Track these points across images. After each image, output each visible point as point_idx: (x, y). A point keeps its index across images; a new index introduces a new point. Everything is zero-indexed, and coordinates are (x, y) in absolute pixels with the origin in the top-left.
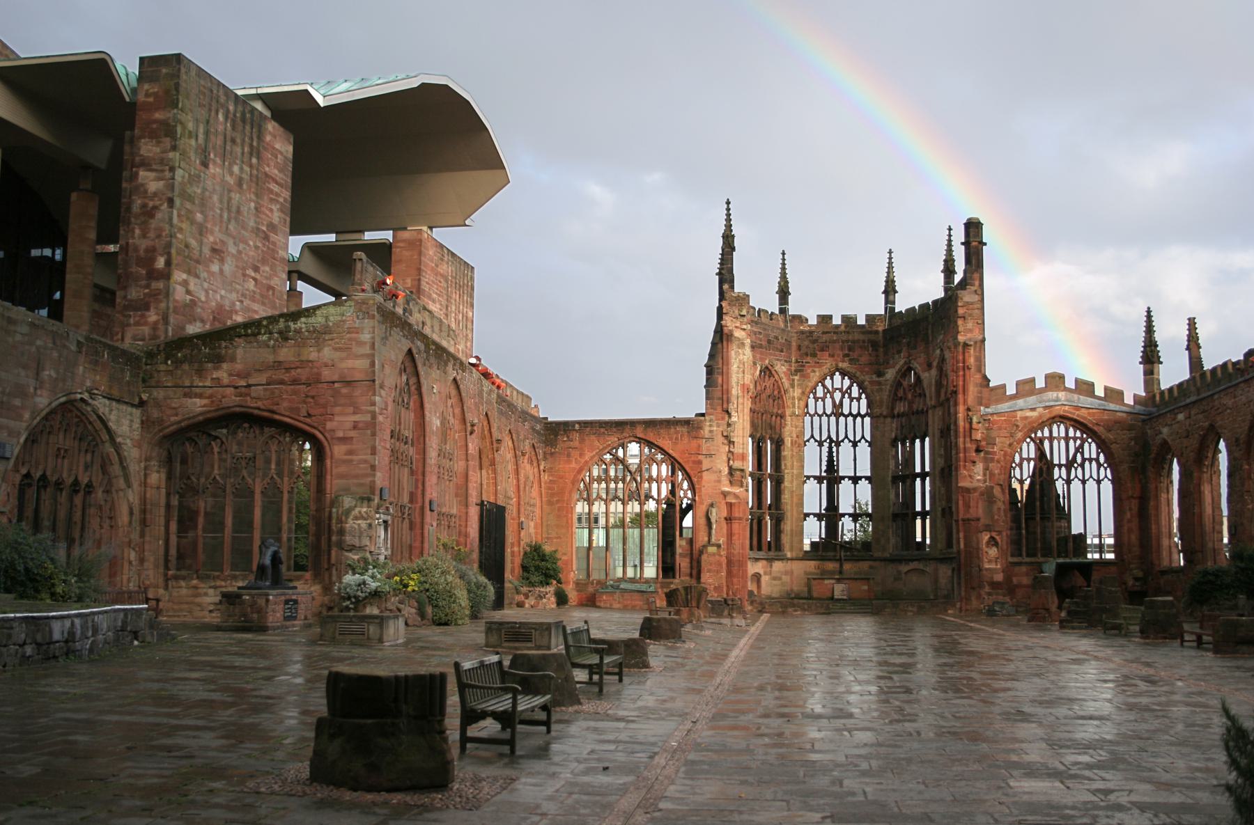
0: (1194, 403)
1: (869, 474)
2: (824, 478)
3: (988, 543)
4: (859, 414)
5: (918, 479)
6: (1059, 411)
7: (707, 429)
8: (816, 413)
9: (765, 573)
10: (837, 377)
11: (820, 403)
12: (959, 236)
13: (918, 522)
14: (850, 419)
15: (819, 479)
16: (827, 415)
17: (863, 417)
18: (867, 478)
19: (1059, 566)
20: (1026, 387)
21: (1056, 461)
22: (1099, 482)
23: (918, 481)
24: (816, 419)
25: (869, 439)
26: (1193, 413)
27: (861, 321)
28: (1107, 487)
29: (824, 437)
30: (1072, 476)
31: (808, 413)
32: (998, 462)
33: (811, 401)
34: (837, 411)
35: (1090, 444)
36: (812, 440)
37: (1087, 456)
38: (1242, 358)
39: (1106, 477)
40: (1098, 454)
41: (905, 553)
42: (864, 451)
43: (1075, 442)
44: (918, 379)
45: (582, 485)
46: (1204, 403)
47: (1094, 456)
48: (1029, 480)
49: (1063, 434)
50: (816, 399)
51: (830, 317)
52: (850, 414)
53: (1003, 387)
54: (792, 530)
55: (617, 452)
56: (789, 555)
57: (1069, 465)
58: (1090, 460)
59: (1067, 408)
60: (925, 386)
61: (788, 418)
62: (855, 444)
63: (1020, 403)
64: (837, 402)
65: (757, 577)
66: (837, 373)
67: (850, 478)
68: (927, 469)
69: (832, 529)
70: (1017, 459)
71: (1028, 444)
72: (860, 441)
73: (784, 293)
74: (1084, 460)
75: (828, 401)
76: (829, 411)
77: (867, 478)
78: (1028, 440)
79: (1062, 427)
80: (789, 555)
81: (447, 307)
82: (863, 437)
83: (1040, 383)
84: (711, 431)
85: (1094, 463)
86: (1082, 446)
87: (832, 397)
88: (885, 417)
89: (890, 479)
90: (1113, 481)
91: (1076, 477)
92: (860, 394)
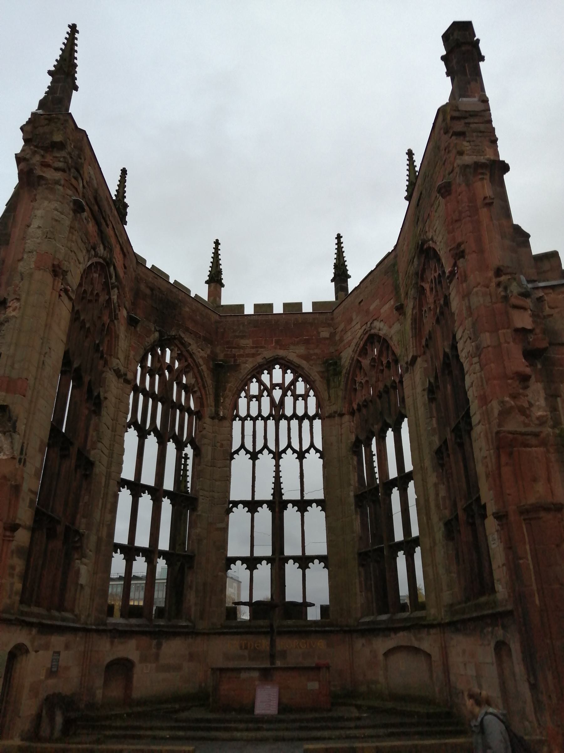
1: (320, 496)
4: (306, 416)
9: (144, 659)
10: (277, 372)
13: (401, 560)
14: (294, 423)
16: (263, 418)
17: (311, 419)
18: (319, 502)
24: (249, 424)
27: (307, 308)
31: (237, 415)
33: (242, 402)
34: (277, 411)
36: (242, 452)
50: (250, 398)
52: (295, 416)
62: (301, 455)
64: (277, 400)
66: (277, 367)
72: (308, 451)
75: (265, 401)
76: (266, 412)
82: (312, 445)
87: (270, 395)
88: (341, 415)
89: (352, 500)
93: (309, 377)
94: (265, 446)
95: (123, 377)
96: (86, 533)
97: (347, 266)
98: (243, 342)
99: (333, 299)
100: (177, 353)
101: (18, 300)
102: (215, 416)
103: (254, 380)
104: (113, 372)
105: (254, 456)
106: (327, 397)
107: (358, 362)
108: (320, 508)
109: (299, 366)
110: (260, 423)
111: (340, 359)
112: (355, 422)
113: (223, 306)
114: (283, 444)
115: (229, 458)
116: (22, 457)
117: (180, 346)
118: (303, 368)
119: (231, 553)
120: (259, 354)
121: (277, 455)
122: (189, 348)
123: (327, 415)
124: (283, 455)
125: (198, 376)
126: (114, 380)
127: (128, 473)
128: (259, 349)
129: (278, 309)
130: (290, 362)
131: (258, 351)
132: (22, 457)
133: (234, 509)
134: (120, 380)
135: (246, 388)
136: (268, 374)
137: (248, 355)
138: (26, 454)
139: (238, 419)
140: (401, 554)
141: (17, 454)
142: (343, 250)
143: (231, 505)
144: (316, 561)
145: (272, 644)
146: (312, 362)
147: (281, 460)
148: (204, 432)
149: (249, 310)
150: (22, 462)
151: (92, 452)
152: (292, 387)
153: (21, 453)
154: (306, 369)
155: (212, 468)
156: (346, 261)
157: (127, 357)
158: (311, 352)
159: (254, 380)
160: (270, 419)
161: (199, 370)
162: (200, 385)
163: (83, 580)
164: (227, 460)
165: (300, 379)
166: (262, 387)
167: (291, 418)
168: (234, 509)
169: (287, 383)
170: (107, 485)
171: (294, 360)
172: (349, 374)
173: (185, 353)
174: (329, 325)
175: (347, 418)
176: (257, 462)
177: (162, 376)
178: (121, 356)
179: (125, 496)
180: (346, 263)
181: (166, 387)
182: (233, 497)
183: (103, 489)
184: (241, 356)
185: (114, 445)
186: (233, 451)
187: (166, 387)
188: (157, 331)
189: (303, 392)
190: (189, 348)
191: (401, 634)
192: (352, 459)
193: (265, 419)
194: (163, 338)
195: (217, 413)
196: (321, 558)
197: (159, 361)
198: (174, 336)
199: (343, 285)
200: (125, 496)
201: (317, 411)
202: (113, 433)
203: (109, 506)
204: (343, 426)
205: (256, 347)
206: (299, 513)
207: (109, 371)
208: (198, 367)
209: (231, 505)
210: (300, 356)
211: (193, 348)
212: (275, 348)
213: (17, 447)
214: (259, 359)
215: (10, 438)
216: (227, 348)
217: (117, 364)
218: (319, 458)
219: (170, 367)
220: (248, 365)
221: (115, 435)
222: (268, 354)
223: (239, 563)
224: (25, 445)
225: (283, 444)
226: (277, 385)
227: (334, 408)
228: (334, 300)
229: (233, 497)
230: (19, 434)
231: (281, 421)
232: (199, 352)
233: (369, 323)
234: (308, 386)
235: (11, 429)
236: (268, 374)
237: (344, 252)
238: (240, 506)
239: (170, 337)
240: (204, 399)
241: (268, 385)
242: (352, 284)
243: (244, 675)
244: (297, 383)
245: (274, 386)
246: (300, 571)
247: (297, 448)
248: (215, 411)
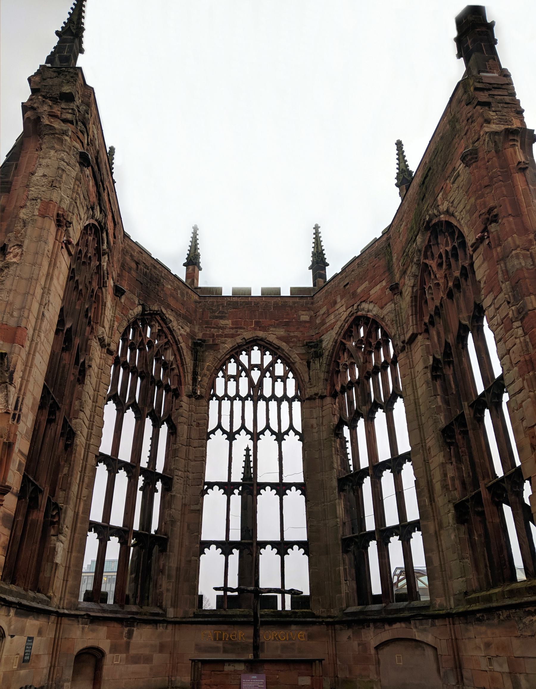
4: (285, 397)
10: (256, 353)
14: (273, 404)
16: (241, 399)
17: (290, 401)
18: (298, 486)
24: (226, 404)
25: (300, 430)
31: (215, 395)
33: (220, 382)
36: (219, 431)
50: (227, 378)
52: (273, 397)
54: (178, 569)
61: (185, 398)
62: (280, 437)
66: (256, 348)
67: (273, 486)
72: (287, 433)
76: (244, 392)
77: (298, 486)
80: (171, 613)
82: (291, 427)
87: (248, 375)
93: (289, 359)
94: (243, 427)
95: (107, 347)
96: (65, 506)
97: (324, 254)
98: (222, 322)
99: (311, 285)
100: (158, 329)
102: (193, 395)
103: (232, 360)
104: (98, 341)
105: (231, 436)
106: (307, 380)
107: (342, 343)
108: (299, 492)
109: (279, 348)
111: (321, 341)
112: (337, 404)
114: (261, 426)
115: (205, 437)
116: (17, 412)
117: (161, 322)
118: (283, 350)
119: (204, 537)
120: (239, 335)
121: (255, 436)
122: (170, 325)
123: (307, 397)
124: (261, 436)
125: (177, 353)
126: (98, 349)
128: (239, 330)
130: (270, 344)
131: (237, 332)
132: (17, 412)
133: (209, 491)
134: (103, 350)
135: (224, 367)
136: (246, 355)
137: (227, 336)
138: (21, 410)
139: (214, 398)
141: (11, 408)
142: (321, 239)
143: (206, 487)
144: (296, 547)
145: (256, 635)
146: (292, 345)
147: (259, 441)
148: (181, 410)
150: (16, 418)
151: (74, 421)
152: (271, 368)
153: (16, 408)
154: (286, 350)
155: (187, 447)
156: (324, 250)
157: (111, 327)
158: (292, 334)
160: (248, 400)
161: (178, 347)
162: (179, 362)
163: (59, 559)
164: (203, 439)
166: (240, 368)
167: (270, 399)
168: (209, 491)
169: (265, 365)
170: (86, 459)
171: (274, 342)
172: (332, 357)
173: (165, 330)
174: (309, 309)
175: (328, 400)
176: (234, 442)
177: (142, 350)
178: (107, 325)
179: (102, 471)
180: (324, 252)
181: (146, 362)
182: (209, 477)
183: (81, 462)
184: (221, 336)
185: (94, 417)
186: (209, 430)
187: (146, 362)
188: (140, 304)
189: (282, 374)
190: (170, 325)
192: (335, 441)
193: (243, 400)
194: (146, 313)
195: (194, 392)
196: (301, 544)
197: (141, 335)
198: (157, 311)
199: (322, 272)
200: (102, 471)
201: (296, 393)
202: (94, 404)
203: (86, 480)
204: (324, 408)
205: (236, 328)
207: (94, 339)
208: (177, 345)
209: (206, 487)
210: (280, 338)
211: (175, 325)
212: (255, 329)
213: (12, 400)
214: (239, 340)
215: (6, 391)
216: (206, 327)
217: (103, 333)
218: (299, 440)
219: (150, 344)
220: (228, 345)
221: (96, 406)
222: (248, 335)
223: (213, 547)
224: (20, 399)
225: (261, 426)
226: (256, 366)
227: (314, 390)
228: (312, 286)
229: (209, 477)
230: (15, 388)
231: (259, 402)
232: (179, 329)
234: (287, 368)
235: (8, 380)
236: (246, 355)
237: (322, 241)
238: (216, 488)
239: (152, 312)
240: (182, 377)
241: (247, 366)
242: (330, 272)
243: (228, 668)
246: (279, 557)
247: (276, 429)
248: (193, 389)
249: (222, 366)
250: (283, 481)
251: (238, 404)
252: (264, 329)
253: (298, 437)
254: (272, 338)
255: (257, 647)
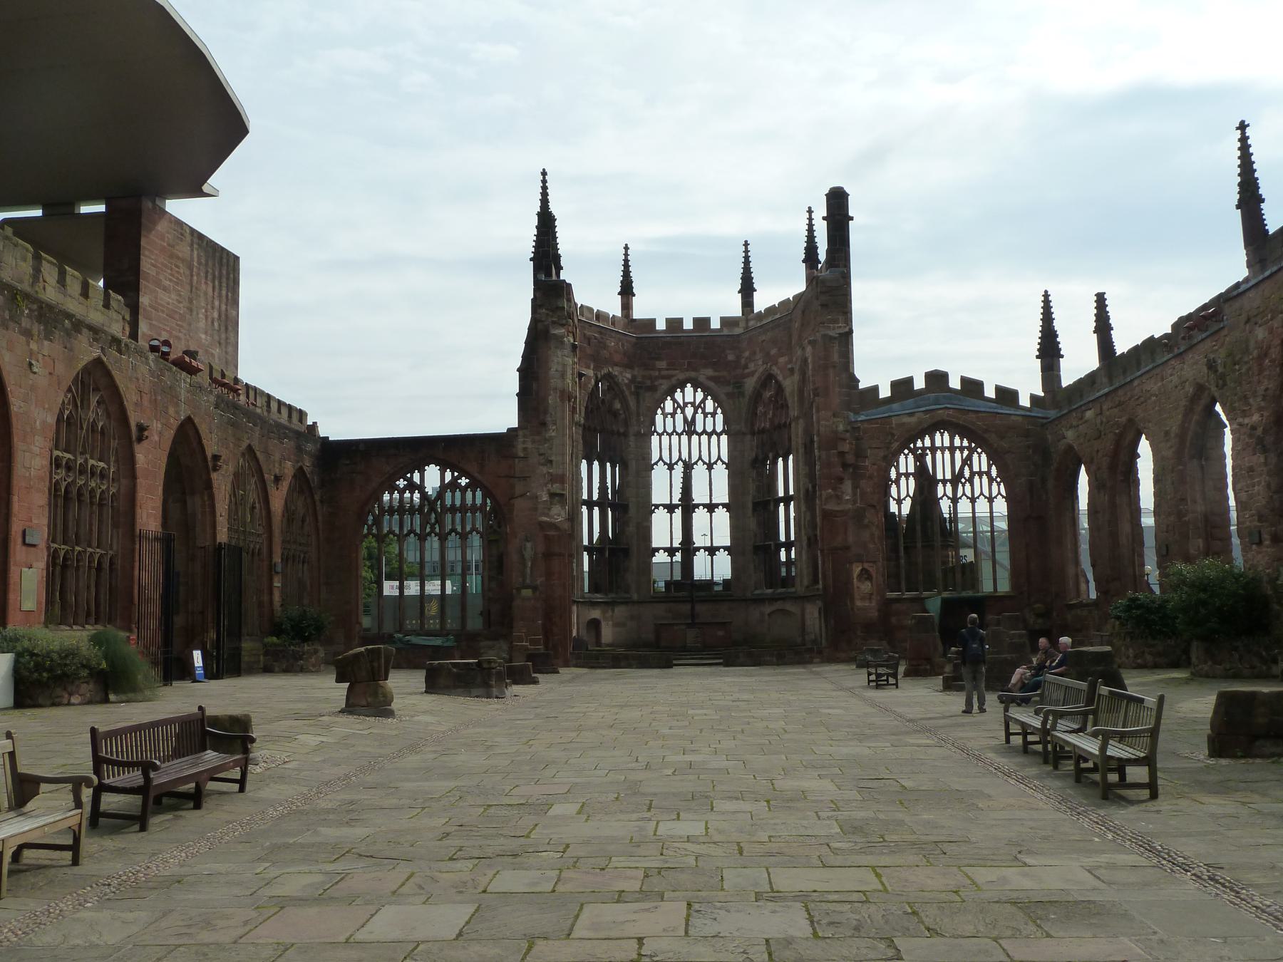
0: (1106, 395)
2: (677, 506)
3: (860, 576)
4: (714, 432)
5: (782, 506)
6: (942, 414)
7: (520, 446)
8: (665, 431)
10: (689, 389)
11: (669, 419)
12: (821, 211)
14: (704, 438)
15: (670, 508)
16: (677, 434)
17: (719, 435)
18: (724, 505)
19: (945, 602)
20: (902, 387)
21: (940, 476)
22: (991, 500)
23: (782, 507)
24: (665, 438)
26: (1105, 407)
27: (715, 325)
28: (1001, 506)
29: (675, 457)
30: (959, 496)
31: (655, 431)
32: (871, 477)
33: (659, 418)
34: (689, 427)
35: (979, 454)
37: (976, 469)
38: (1169, 331)
39: (999, 493)
40: (989, 467)
41: (770, 591)
42: (721, 475)
43: (962, 453)
44: (780, 389)
45: (371, 518)
46: (1120, 392)
47: (984, 468)
48: (909, 500)
49: (947, 443)
50: (665, 415)
51: (680, 321)
52: (704, 432)
53: (875, 389)
55: (412, 476)
56: (635, 597)
57: (956, 479)
58: (980, 474)
59: (951, 412)
60: (787, 394)
61: (632, 438)
62: (710, 467)
63: (895, 406)
65: (595, 625)
66: (689, 385)
67: (705, 506)
68: (791, 493)
69: (687, 565)
70: (893, 475)
71: (906, 456)
72: (715, 463)
73: (627, 290)
74: (973, 474)
75: (679, 417)
76: (680, 429)
77: (724, 505)
78: (906, 451)
79: (946, 435)
81: (191, 301)
82: (719, 458)
83: (919, 384)
84: (525, 449)
85: (985, 478)
86: (970, 457)
87: (683, 412)
88: (744, 434)
89: (750, 505)
90: (1008, 499)
91: (964, 494)
92: (715, 410)
101: (555, 424)
103: (669, 398)
110: (675, 438)
113: (635, 320)
114: (695, 458)
119: (654, 545)
127: (585, 496)
129: (688, 325)
133: (656, 510)
137: (664, 377)
140: (783, 549)
143: (653, 507)
145: (693, 608)
149: (661, 326)
152: (702, 405)
159: (669, 398)
165: (709, 398)
166: (676, 405)
168: (656, 510)
169: (697, 404)
176: (673, 471)
179: (584, 509)
184: (657, 378)
186: (653, 463)
191: (779, 602)
193: (679, 435)
206: (708, 514)
210: (710, 378)
214: (674, 381)
220: (665, 385)
222: (681, 376)
223: (661, 551)
233: (769, 364)
238: (661, 508)
241: (682, 405)
243: (676, 628)
244: (707, 401)
245: (686, 404)
249: (660, 402)
250: (713, 502)
251: (675, 438)
252: (695, 370)
253: (724, 466)
254: (702, 379)
255: (693, 616)
